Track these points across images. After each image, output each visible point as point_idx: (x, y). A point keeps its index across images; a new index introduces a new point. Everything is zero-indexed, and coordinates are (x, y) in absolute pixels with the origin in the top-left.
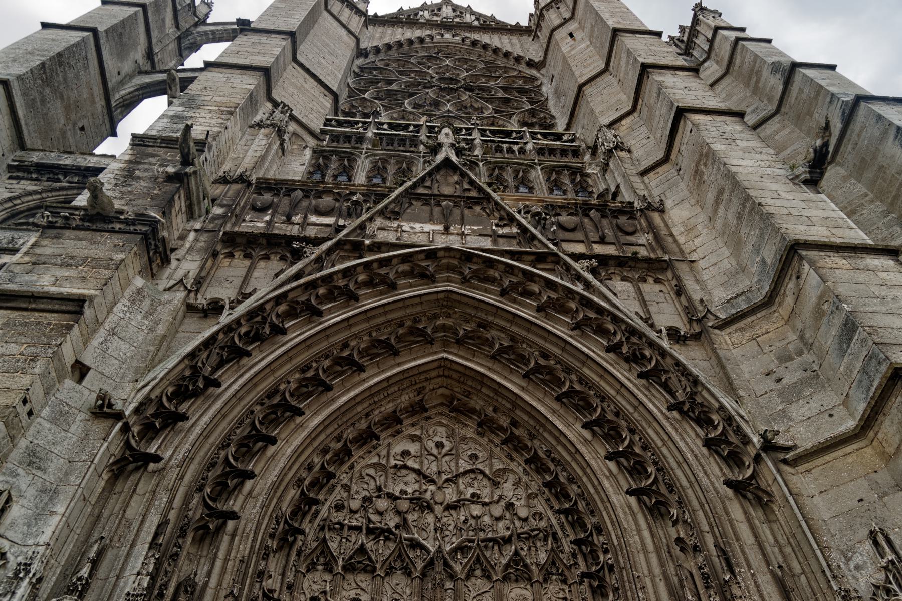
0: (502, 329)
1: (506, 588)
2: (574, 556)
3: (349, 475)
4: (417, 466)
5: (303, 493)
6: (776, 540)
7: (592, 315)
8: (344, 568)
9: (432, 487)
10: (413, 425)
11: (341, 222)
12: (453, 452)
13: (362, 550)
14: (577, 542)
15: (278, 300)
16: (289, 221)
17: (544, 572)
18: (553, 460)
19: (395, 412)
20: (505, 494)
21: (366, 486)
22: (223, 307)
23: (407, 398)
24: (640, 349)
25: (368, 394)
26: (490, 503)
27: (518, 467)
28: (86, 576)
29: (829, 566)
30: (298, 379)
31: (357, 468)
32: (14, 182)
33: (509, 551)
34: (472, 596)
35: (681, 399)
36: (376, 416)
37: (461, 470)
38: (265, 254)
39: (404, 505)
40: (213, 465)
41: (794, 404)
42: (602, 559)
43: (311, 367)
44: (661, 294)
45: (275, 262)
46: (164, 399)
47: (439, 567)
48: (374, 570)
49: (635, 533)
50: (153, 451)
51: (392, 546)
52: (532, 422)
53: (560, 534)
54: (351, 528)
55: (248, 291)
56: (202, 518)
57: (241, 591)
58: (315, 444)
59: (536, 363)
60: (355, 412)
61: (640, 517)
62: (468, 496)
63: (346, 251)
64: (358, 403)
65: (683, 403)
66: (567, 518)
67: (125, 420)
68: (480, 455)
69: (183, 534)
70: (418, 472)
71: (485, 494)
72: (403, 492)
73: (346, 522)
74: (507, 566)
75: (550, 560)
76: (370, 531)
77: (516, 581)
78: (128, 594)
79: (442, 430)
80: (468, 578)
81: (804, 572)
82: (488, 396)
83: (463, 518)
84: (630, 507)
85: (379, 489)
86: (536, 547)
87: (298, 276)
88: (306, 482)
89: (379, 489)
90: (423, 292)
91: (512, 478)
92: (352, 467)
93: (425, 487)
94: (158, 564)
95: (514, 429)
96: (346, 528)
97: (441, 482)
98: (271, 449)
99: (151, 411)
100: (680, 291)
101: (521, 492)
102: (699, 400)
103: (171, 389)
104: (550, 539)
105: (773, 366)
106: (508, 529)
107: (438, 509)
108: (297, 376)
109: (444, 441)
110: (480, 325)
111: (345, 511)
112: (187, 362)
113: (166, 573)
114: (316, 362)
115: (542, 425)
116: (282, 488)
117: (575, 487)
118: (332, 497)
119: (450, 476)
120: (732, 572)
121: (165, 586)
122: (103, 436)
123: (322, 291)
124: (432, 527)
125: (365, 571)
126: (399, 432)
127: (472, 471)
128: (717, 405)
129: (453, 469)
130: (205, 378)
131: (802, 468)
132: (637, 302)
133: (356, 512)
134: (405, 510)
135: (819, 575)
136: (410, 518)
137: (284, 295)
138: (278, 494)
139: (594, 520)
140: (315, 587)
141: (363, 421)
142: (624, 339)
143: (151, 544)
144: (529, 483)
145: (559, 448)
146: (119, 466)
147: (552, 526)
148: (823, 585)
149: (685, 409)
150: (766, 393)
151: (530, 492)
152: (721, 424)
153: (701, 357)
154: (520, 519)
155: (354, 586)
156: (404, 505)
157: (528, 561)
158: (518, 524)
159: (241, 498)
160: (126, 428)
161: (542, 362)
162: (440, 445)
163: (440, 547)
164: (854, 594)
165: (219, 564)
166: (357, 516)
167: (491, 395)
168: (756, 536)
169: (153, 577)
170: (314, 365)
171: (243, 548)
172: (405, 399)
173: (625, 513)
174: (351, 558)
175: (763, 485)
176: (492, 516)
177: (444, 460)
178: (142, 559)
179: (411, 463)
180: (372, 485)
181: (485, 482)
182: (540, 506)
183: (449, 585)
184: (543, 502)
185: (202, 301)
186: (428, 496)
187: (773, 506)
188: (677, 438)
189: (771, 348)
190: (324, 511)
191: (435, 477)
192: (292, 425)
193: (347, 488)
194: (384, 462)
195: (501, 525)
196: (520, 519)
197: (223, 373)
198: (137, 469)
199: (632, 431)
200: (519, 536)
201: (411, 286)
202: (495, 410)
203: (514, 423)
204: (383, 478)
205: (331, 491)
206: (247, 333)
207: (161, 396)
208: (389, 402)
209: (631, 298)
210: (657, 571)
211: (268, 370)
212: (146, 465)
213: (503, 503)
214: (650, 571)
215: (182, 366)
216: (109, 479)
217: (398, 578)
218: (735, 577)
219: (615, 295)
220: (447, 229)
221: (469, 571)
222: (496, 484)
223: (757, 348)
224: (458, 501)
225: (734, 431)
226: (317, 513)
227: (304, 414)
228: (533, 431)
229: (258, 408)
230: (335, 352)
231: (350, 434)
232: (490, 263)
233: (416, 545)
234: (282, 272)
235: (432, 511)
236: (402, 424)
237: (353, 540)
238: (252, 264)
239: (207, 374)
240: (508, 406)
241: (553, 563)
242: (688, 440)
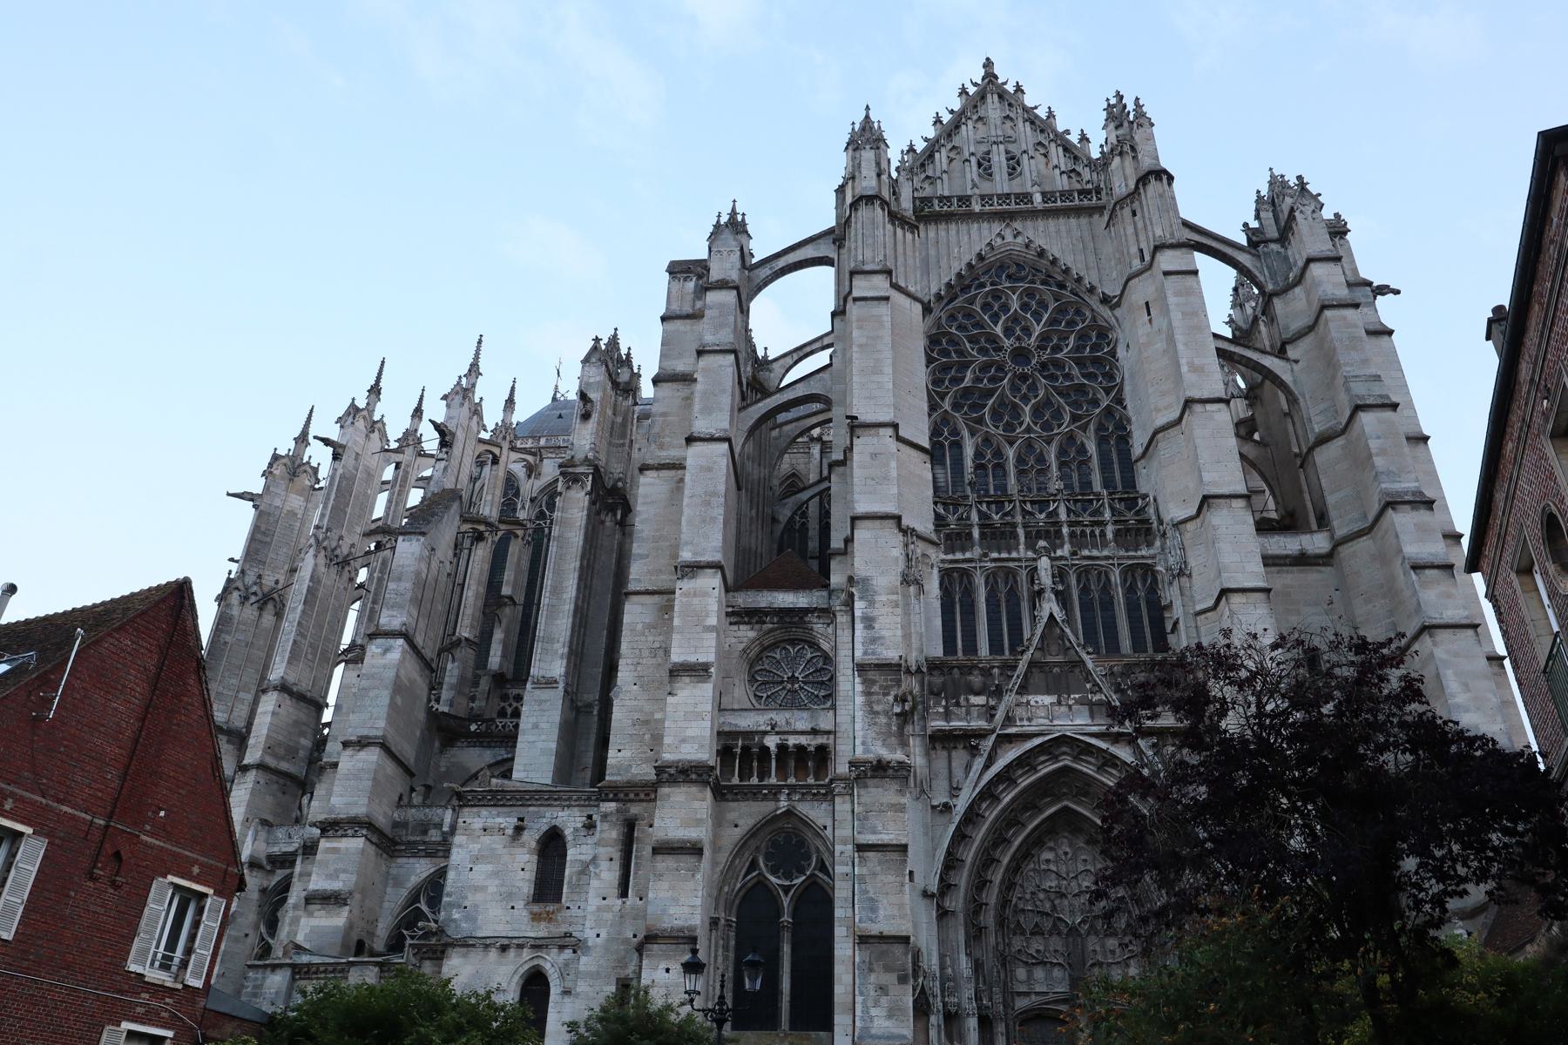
4: (1054, 869)
9: (1065, 882)
11: (992, 703)
16: (958, 704)
32: (735, 628)
48: (1043, 934)
72: (1050, 887)
76: (1038, 912)
79: (1065, 840)
109: (1068, 850)
136: (1056, 902)
193: (1022, 886)
194: (1037, 867)
217: (1054, 938)
220: (1059, 703)
233: (1060, 919)
235: (1066, 897)
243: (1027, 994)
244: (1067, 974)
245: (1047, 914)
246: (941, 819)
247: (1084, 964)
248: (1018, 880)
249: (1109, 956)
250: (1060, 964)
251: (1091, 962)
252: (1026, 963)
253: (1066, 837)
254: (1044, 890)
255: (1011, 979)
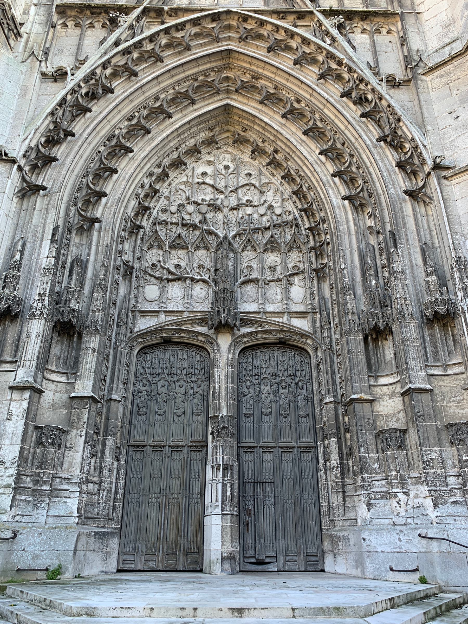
0: (269, 79)
1: (266, 255)
2: (308, 236)
3: (169, 189)
4: (211, 182)
5: (140, 203)
6: (429, 227)
7: (334, 66)
8: (170, 247)
9: (222, 196)
10: (209, 153)
12: (235, 172)
13: (179, 235)
14: (310, 229)
15: (104, 66)
17: (288, 246)
18: (300, 176)
19: (195, 145)
20: (268, 199)
21: (180, 197)
22: (66, 73)
23: (204, 135)
24: (365, 94)
25: (176, 134)
26: (258, 206)
27: (277, 180)
28: (19, 259)
29: (453, 243)
30: (127, 126)
31: (173, 185)
33: (268, 234)
34: (245, 261)
35: (387, 133)
36: (183, 148)
37: (240, 184)
38: (91, 23)
39: (204, 209)
40: (80, 189)
41: (462, 136)
42: (324, 238)
43: (135, 116)
44: (390, 44)
45: (99, 30)
46: (40, 147)
47: (226, 246)
48: (187, 248)
49: (345, 223)
50: (40, 184)
51: (197, 233)
52: (287, 150)
53: (300, 223)
54: (172, 223)
55: (82, 58)
56: (79, 223)
57: (109, 263)
58: (144, 171)
59: (292, 105)
60: (168, 147)
61: (350, 213)
62: (244, 202)
63: (151, 18)
64: (170, 141)
65: (387, 136)
66: (306, 213)
67: (18, 164)
68: (253, 173)
69: (70, 232)
70: (213, 186)
71: (255, 198)
72: (203, 200)
73: (169, 220)
74: (266, 244)
75: (293, 240)
76: (183, 225)
77: (272, 252)
78: (44, 268)
79: (228, 156)
80: (243, 251)
81: (439, 246)
82: (259, 131)
83: (240, 216)
84: (344, 206)
85: (188, 198)
86: (285, 232)
87: (117, 44)
88: (142, 196)
89: (188, 198)
90: (210, 52)
91: (273, 188)
92: (170, 184)
93: (217, 197)
94: (58, 252)
95: (275, 154)
96: (169, 224)
97: (227, 193)
98: (115, 176)
99: (33, 156)
100: (403, 41)
101: (278, 198)
102: (399, 132)
103: (43, 140)
104: (294, 227)
105: (455, 107)
106: (268, 221)
107: (226, 210)
108: (126, 123)
110: (252, 78)
111: (168, 213)
112: (49, 118)
113: (64, 254)
114: (138, 112)
115: (294, 152)
116: (126, 201)
117: (312, 193)
118: (159, 205)
119: (233, 189)
120: (396, 247)
121: (65, 262)
122: (7, 175)
123: (135, 55)
124: (222, 222)
125: (182, 248)
126: (199, 159)
127: (247, 185)
128: (411, 137)
129: (235, 183)
130: (64, 130)
131: (454, 181)
132: (370, 53)
133: (174, 214)
134: (205, 212)
135: (447, 248)
136: (208, 216)
137: (109, 61)
138: (124, 204)
139: (322, 214)
140: (154, 258)
141: (175, 153)
142: (354, 86)
143: (51, 240)
144: (284, 191)
145: (304, 168)
146: (22, 193)
147: (296, 219)
148: (448, 254)
149: (389, 140)
150: (446, 127)
151: (284, 197)
152: (410, 151)
153: (408, 99)
154: (276, 215)
155: (177, 257)
156: (204, 209)
157: (279, 241)
158: (274, 217)
159: (100, 209)
160: (20, 169)
161: (296, 105)
162: (227, 167)
163: (226, 234)
164: (463, 259)
165: (93, 248)
166: (175, 216)
167: (261, 130)
168: (417, 225)
169: (57, 259)
170: (137, 114)
171: (107, 240)
172: (202, 136)
173: (340, 211)
174: (173, 241)
175: (428, 191)
176: (259, 214)
177: (229, 178)
178: (48, 249)
179: (208, 180)
180: (184, 197)
181: (256, 192)
182: (290, 207)
183: (232, 255)
184: (292, 204)
185: (50, 69)
186: (219, 202)
187: (431, 206)
188: (380, 162)
189: (458, 92)
190: (155, 213)
191: (223, 190)
192: (127, 159)
193: (167, 198)
195: (264, 218)
196: (276, 215)
197: (75, 126)
198: (34, 194)
199: (351, 156)
200: (274, 226)
201: (201, 45)
202: (264, 141)
203: (276, 151)
204: (190, 191)
205: (158, 201)
206: (87, 94)
207: (38, 146)
208: (191, 138)
209: (366, 49)
210: (355, 246)
211: (105, 121)
212: (39, 191)
213: (266, 205)
214: (351, 246)
215: (47, 122)
216: (18, 201)
217: (202, 252)
218: (397, 250)
219: (353, 47)
221: (243, 248)
222: (262, 193)
223: (448, 91)
224: (238, 205)
225: (418, 156)
226: (150, 215)
227: (133, 151)
228: (288, 157)
229: (103, 148)
230: (150, 104)
231: (166, 162)
232: (262, 23)
233: (210, 233)
234: (105, 39)
236: (200, 154)
237: (174, 231)
238: (82, 32)
239: (64, 128)
240: (272, 138)
241: (295, 241)
242: (387, 163)
243: (154, 313)
244: (211, 290)
245: (194, 227)
246: (51, 87)
247: (235, 281)
248: (163, 188)
249: (268, 272)
250: (204, 281)
251: (242, 279)
252: (159, 279)
253: (227, 152)
254: (195, 203)
255: (136, 297)
